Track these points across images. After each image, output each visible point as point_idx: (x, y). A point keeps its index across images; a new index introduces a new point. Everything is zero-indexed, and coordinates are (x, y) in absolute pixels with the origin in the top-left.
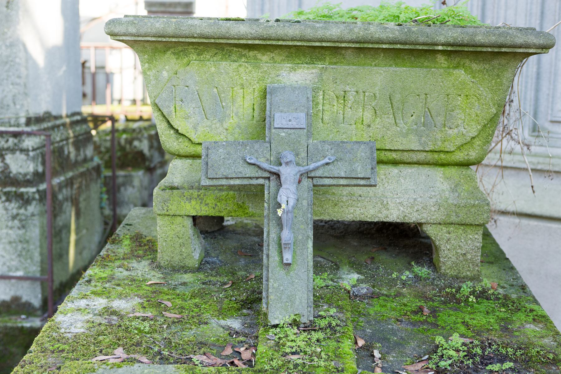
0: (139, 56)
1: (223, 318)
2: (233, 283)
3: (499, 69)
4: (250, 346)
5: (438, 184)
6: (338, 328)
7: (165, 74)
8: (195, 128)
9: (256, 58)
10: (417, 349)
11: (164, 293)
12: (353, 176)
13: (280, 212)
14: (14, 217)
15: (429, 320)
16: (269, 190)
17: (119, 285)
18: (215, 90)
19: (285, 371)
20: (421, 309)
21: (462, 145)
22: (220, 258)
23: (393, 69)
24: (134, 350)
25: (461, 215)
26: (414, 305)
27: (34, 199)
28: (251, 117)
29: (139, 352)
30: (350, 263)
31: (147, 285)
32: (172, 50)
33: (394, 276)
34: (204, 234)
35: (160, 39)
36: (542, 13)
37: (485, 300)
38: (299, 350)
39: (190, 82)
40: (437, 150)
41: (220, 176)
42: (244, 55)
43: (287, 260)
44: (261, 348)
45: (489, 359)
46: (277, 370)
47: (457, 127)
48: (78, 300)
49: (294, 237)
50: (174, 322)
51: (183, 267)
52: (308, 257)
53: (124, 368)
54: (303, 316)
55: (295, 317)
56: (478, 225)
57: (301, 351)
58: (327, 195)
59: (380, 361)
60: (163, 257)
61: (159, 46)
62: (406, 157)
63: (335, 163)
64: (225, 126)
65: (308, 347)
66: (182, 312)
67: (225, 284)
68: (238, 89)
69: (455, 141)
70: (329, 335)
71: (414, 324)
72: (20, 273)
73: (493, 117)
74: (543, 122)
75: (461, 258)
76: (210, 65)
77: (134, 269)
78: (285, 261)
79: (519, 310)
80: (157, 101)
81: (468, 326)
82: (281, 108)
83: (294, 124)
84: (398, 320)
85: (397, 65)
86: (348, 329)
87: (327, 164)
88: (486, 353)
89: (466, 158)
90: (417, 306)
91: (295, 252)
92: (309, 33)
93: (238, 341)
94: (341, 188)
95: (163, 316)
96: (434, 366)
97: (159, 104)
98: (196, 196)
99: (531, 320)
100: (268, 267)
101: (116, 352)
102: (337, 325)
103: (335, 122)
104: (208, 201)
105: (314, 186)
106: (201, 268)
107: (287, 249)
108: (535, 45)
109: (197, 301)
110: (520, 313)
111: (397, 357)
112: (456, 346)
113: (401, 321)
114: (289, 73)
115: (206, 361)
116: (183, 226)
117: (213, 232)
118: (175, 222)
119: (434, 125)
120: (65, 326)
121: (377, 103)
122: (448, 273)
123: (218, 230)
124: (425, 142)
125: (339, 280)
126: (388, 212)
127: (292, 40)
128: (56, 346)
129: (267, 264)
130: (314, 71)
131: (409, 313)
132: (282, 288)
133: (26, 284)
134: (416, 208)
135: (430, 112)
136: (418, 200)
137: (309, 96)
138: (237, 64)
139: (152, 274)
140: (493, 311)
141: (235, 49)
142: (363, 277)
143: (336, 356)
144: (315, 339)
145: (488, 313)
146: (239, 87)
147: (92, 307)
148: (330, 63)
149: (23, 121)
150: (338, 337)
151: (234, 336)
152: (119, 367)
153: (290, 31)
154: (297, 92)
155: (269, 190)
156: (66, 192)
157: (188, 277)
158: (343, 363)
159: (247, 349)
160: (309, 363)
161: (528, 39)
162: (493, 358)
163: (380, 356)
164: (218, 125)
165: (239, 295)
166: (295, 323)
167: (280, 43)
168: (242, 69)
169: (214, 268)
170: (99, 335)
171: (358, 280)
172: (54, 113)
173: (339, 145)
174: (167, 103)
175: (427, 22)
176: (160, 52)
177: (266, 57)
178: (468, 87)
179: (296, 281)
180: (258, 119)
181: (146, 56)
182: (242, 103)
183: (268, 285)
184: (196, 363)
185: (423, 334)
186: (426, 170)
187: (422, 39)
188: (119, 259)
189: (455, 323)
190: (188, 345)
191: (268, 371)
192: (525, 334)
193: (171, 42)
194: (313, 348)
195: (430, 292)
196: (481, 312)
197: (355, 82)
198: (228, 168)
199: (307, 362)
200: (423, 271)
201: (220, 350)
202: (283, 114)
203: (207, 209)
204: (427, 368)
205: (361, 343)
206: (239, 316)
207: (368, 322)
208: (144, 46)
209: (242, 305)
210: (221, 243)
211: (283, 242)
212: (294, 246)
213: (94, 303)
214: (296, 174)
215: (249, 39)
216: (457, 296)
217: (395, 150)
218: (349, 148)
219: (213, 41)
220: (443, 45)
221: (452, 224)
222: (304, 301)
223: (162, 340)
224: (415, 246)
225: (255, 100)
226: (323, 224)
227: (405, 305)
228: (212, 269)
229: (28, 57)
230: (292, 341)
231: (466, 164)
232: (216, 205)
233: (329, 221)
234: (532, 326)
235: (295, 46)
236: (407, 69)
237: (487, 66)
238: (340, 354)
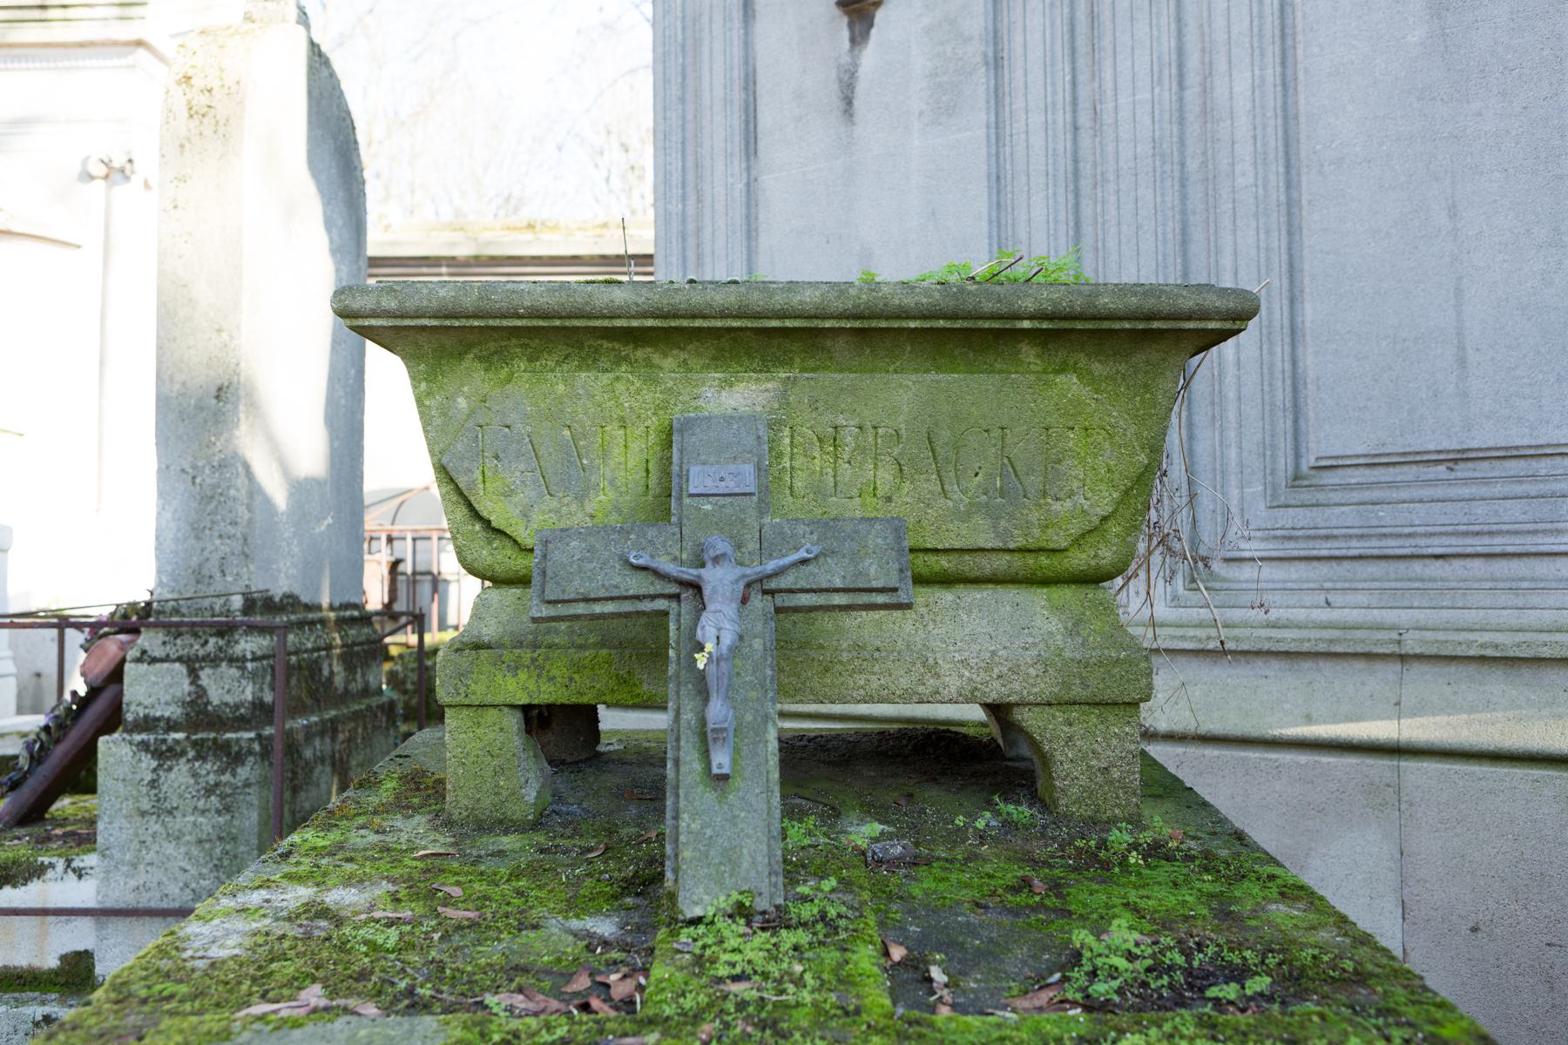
0: (407, 367)
1: (577, 916)
2: (607, 849)
3: (1147, 372)
4: (634, 970)
5: (1039, 622)
6: (842, 923)
7: (462, 403)
8: (525, 515)
9: (649, 363)
10: (1030, 962)
11: (450, 872)
12: (861, 586)
14: (209, 791)
15: (1047, 902)
16: (678, 621)
17: (350, 860)
18: (567, 432)
19: (715, 1017)
20: (1026, 883)
21: (1083, 536)
22: (585, 805)
23: (932, 376)
24: (348, 988)
25: (1092, 682)
26: (1010, 875)
27: (250, 752)
28: (641, 489)
29: (359, 994)
30: (862, 806)
31: (415, 859)
32: (476, 351)
33: (960, 821)
34: (557, 766)
35: (448, 323)
37: (1163, 862)
38: (749, 970)
39: (513, 417)
40: (1032, 547)
41: (572, 596)
42: (626, 359)
43: (720, 766)
44: (659, 971)
45: (1206, 978)
46: (695, 1016)
47: (1071, 495)
48: (247, 891)
49: (736, 718)
50: (459, 928)
51: (501, 822)
52: (767, 761)
53: (309, 1028)
54: (760, 894)
55: (740, 897)
56: (1129, 703)
57: (755, 972)
58: (807, 651)
59: (945, 992)
60: (458, 801)
61: (449, 342)
62: (968, 564)
63: (822, 560)
64: (589, 510)
65: (772, 963)
66: (483, 906)
67: (590, 850)
68: (613, 429)
69: (1069, 526)
70: (821, 937)
71: (1015, 912)
73: (1142, 474)
75: (1100, 779)
76: (555, 380)
77: (393, 829)
78: (715, 771)
79: (1243, 877)
80: (444, 461)
81: (1138, 912)
82: (702, 457)
83: (730, 485)
84: (978, 905)
85: (939, 369)
86: (866, 924)
87: (804, 562)
88: (1196, 964)
89: (1093, 563)
90: (1016, 877)
91: (737, 750)
93: (606, 960)
94: (837, 614)
95: (439, 915)
96: (1079, 996)
97: (450, 467)
98: (528, 662)
99: (1275, 895)
100: (677, 787)
101: (303, 995)
102: (840, 916)
103: (819, 492)
104: (554, 672)
105: (778, 610)
106: (541, 824)
107: (719, 743)
108: (1218, 313)
109: (521, 883)
110: (1246, 884)
111: (986, 981)
112: (1125, 946)
113: (985, 907)
114: (719, 392)
115: (523, 1006)
116: (501, 729)
117: (577, 763)
118: (483, 721)
119: (1022, 493)
120: (197, 944)
121: (904, 449)
122: (1073, 813)
123: (587, 759)
124: (1006, 530)
125: (840, 836)
126: (937, 682)
127: (723, 316)
128: (159, 987)
129: (674, 782)
130: (770, 386)
131: (1000, 891)
132: (709, 832)
134: (996, 671)
135: (1013, 467)
136: (1000, 653)
137: (761, 433)
138: (611, 375)
139: (432, 837)
140: (1187, 881)
141: (606, 344)
142: (891, 829)
143: (840, 981)
144: (788, 945)
145: (1175, 884)
146: (616, 425)
147: (276, 904)
148: (803, 370)
150: (843, 940)
151: (599, 950)
152: (297, 1024)
153: (717, 298)
154: (735, 426)
155: (678, 621)
156: (320, 745)
157: (508, 842)
158: (858, 996)
159: (625, 977)
160: (775, 998)
161: (1205, 299)
162: (1213, 974)
163: (945, 979)
164: (574, 507)
165: (620, 870)
166: (740, 911)
167: (698, 323)
168: (620, 387)
169: (570, 823)
170: (272, 961)
171: (882, 833)
172: (305, 598)
173: (828, 526)
174: (466, 464)
176: (451, 355)
177: (670, 360)
178: (1088, 410)
179: (743, 814)
180: (658, 490)
181: (422, 367)
182: (623, 459)
183: (677, 827)
184: (494, 1010)
185: (1040, 931)
186: (1011, 594)
187: (988, 306)
188: (364, 813)
189: (1108, 907)
190: (485, 973)
191: (672, 1019)
192: (1270, 923)
193: (472, 328)
194: (785, 966)
195: (1039, 852)
196: (1160, 884)
197: (855, 406)
198: (590, 580)
199: (771, 996)
200: (1020, 812)
201: (561, 980)
202: (706, 468)
203: (552, 689)
204: (1062, 1002)
205: (897, 953)
206: (615, 911)
207: (909, 912)
208: (416, 343)
209: (623, 889)
210: (591, 779)
211: (710, 726)
212: (735, 736)
213: (283, 897)
214: (737, 581)
215: (633, 317)
216: (1102, 854)
217: (946, 551)
218: (849, 529)
219: (558, 323)
220: (1031, 318)
221: (1075, 703)
222: (762, 860)
223: (424, 965)
224: (995, 773)
225: (651, 452)
226: (804, 743)
227: (991, 877)
228: (564, 825)
229: (254, 489)
230: (733, 951)
231: (1093, 578)
232: (571, 679)
233: (816, 737)
234: (1281, 906)
235: (730, 330)
236: (962, 376)
237: (1122, 368)
238: (848, 976)
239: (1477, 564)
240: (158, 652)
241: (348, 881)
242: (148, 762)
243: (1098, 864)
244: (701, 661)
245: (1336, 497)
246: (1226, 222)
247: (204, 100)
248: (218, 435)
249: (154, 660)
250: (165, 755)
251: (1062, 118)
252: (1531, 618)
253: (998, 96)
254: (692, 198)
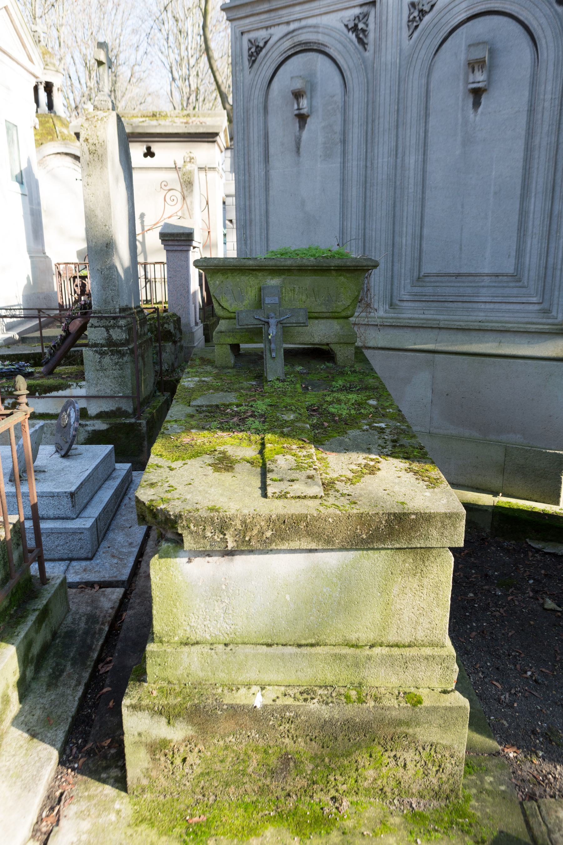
14: (116, 364)
20: (328, 377)
23: (314, 277)
27: (127, 353)
36: (393, 244)
62: (321, 315)
72: (121, 395)
74: (396, 301)
83: (273, 302)
92: (278, 263)
133: (124, 400)
149: (118, 310)
157: (229, 370)
166: (278, 379)
175: (326, 257)
186: (330, 321)
187: (325, 265)
239: (460, 304)
240: (97, 324)
241: (204, 377)
242: (98, 356)
243: (342, 374)
244: (270, 337)
245: (428, 284)
246: (405, 202)
247: (93, 148)
248: (108, 259)
249: (95, 327)
250: (103, 354)
251: (362, 163)
252: (470, 318)
253: (344, 153)
254: (247, 174)
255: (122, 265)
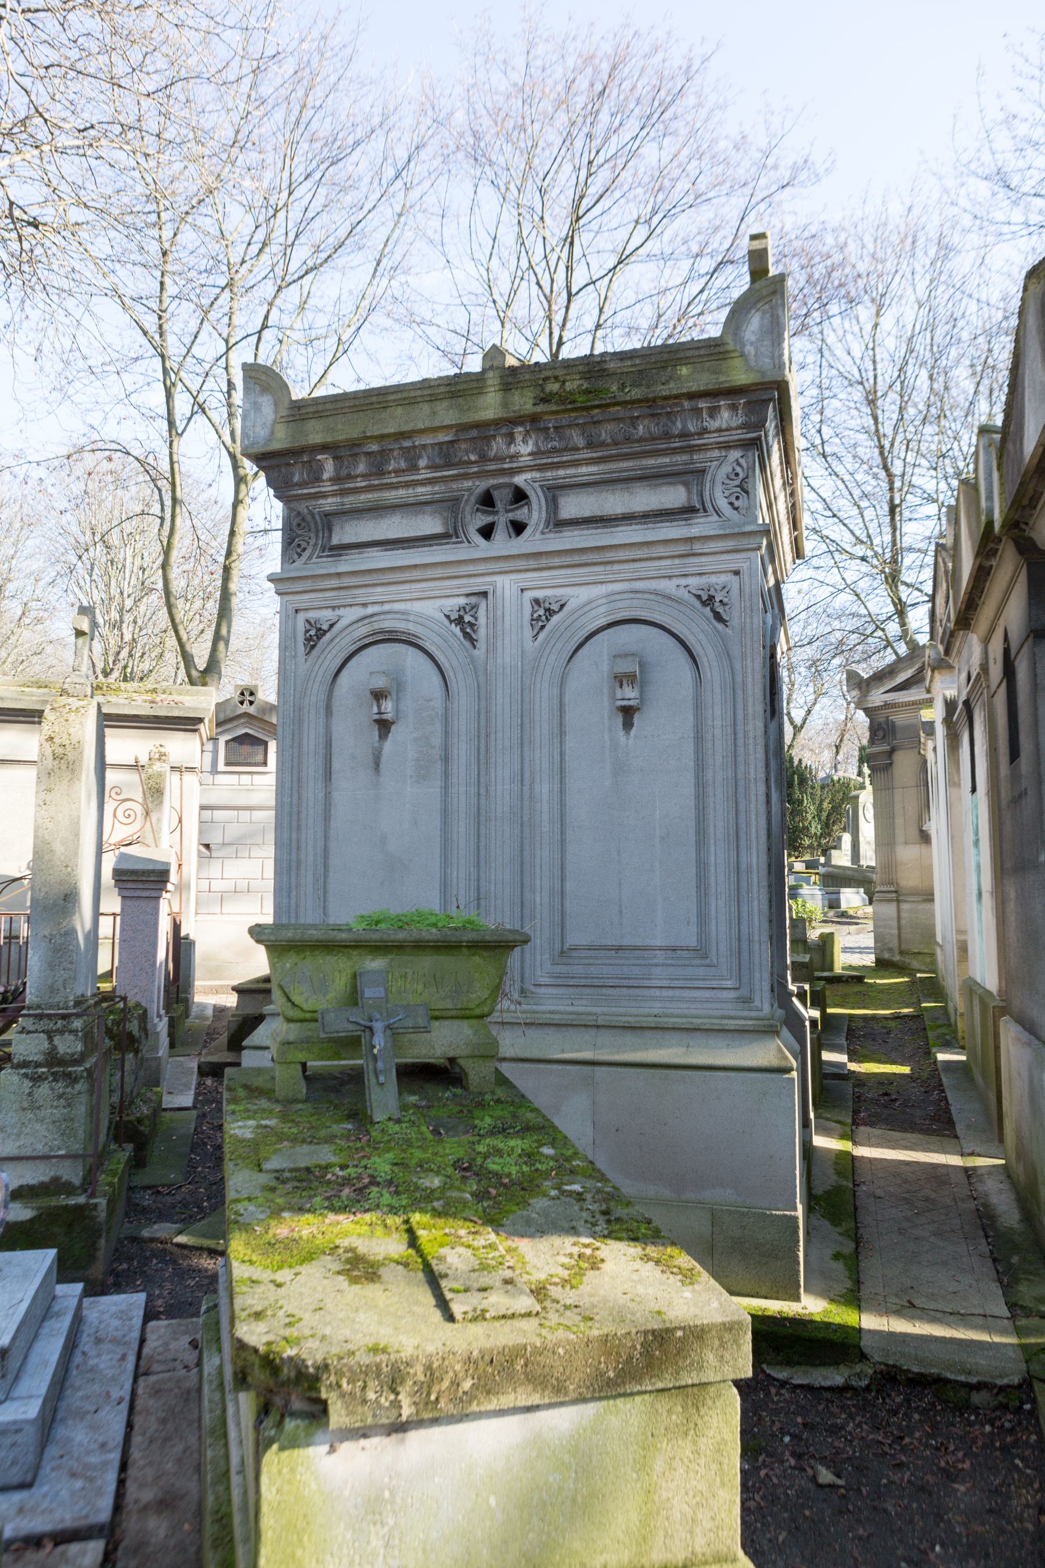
13: (375, 1051)
14: (60, 1097)
20: (461, 1111)
62: (444, 1013)
72: (62, 1152)
74: (528, 986)
83: (377, 995)
92: (385, 937)
103: (399, 992)
133: (67, 1163)
157: (300, 1106)
173: (407, 1007)
186: (457, 1022)
200: (459, 1091)
231: (481, 1017)
239: (624, 990)
240: (32, 1028)
242: (27, 1083)
243: (481, 1105)
245: (576, 961)
246: (538, 845)
247: (61, 750)
248: (64, 919)
249: (29, 1032)
250: (37, 1079)
251: (473, 790)
252: (641, 1011)
253: (446, 775)
254: (296, 795)
255: (83, 927)
